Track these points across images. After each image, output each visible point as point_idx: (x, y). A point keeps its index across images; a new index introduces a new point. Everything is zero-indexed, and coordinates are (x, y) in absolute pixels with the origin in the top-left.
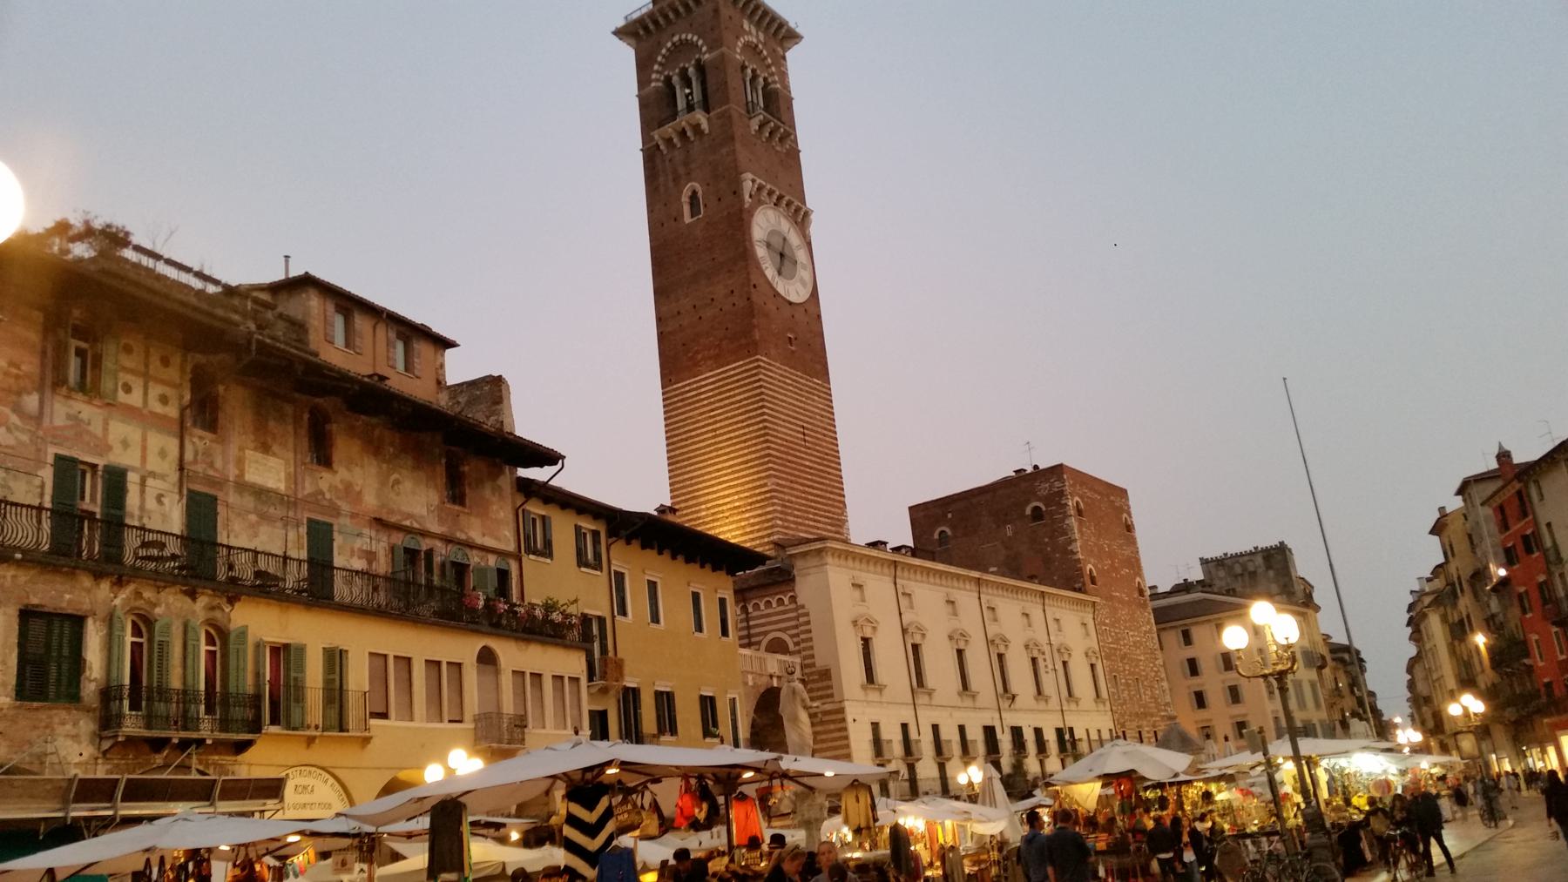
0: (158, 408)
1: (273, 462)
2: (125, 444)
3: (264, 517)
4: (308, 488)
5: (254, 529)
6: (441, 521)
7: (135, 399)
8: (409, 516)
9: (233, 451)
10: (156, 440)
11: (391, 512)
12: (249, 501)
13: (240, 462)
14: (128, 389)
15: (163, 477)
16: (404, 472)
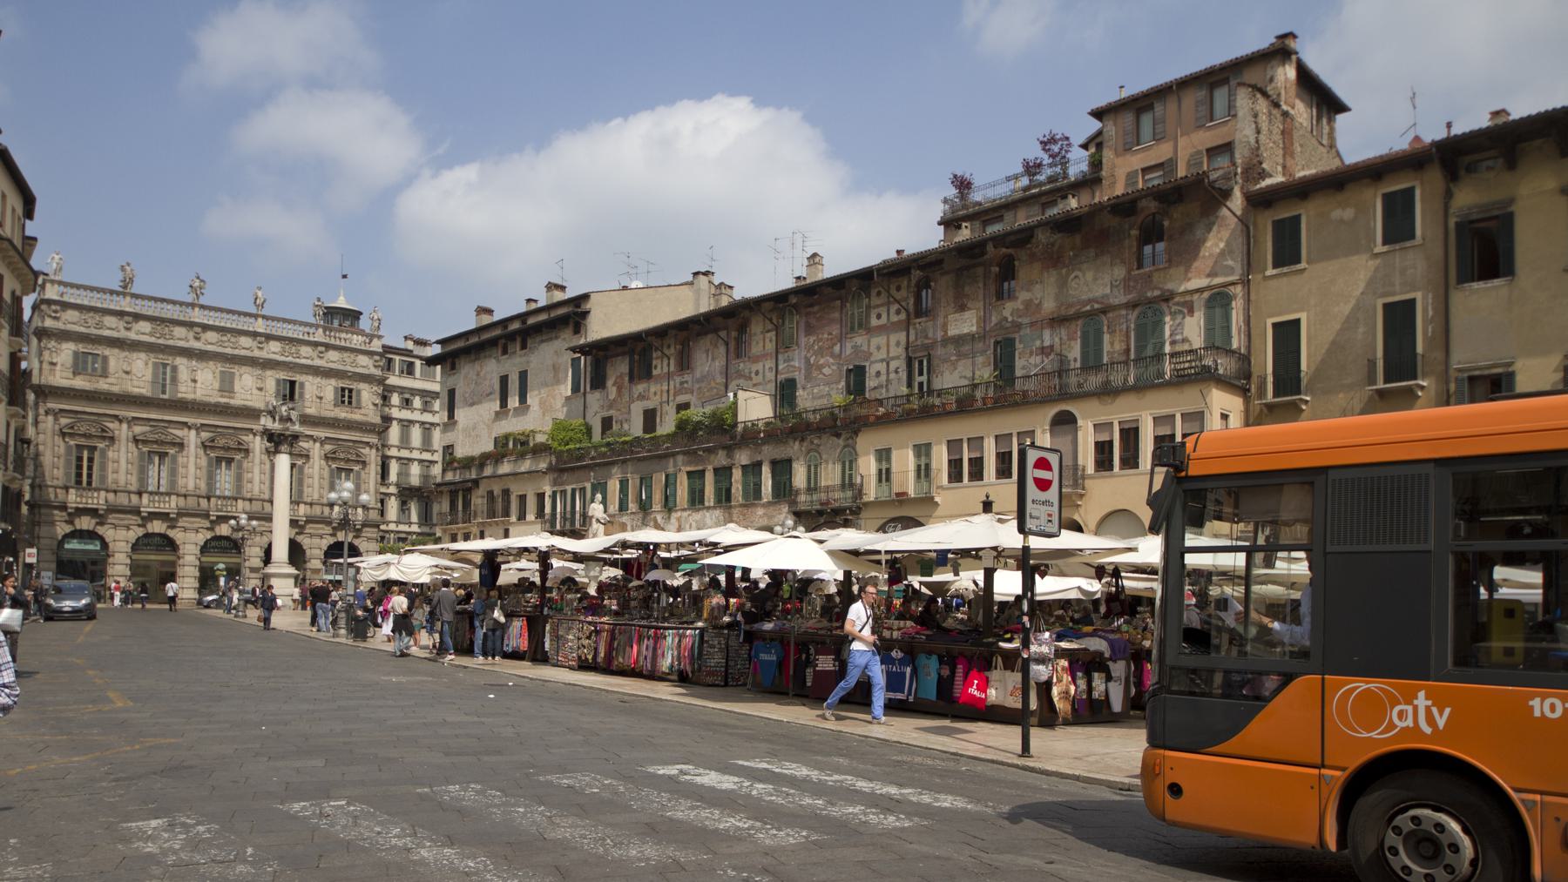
0: (895, 318)
1: (967, 314)
2: (879, 348)
3: (961, 356)
4: (994, 319)
5: (954, 365)
6: (1127, 289)
7: (884, 320)
8: (1090, 301)
9: (940, 320)
10: (894, 338)
11: (1071, 306)
12: (951, 349)
13: (945, 327)
14: (879, 317)
15: (897, 358)
16: (1085, 266)
